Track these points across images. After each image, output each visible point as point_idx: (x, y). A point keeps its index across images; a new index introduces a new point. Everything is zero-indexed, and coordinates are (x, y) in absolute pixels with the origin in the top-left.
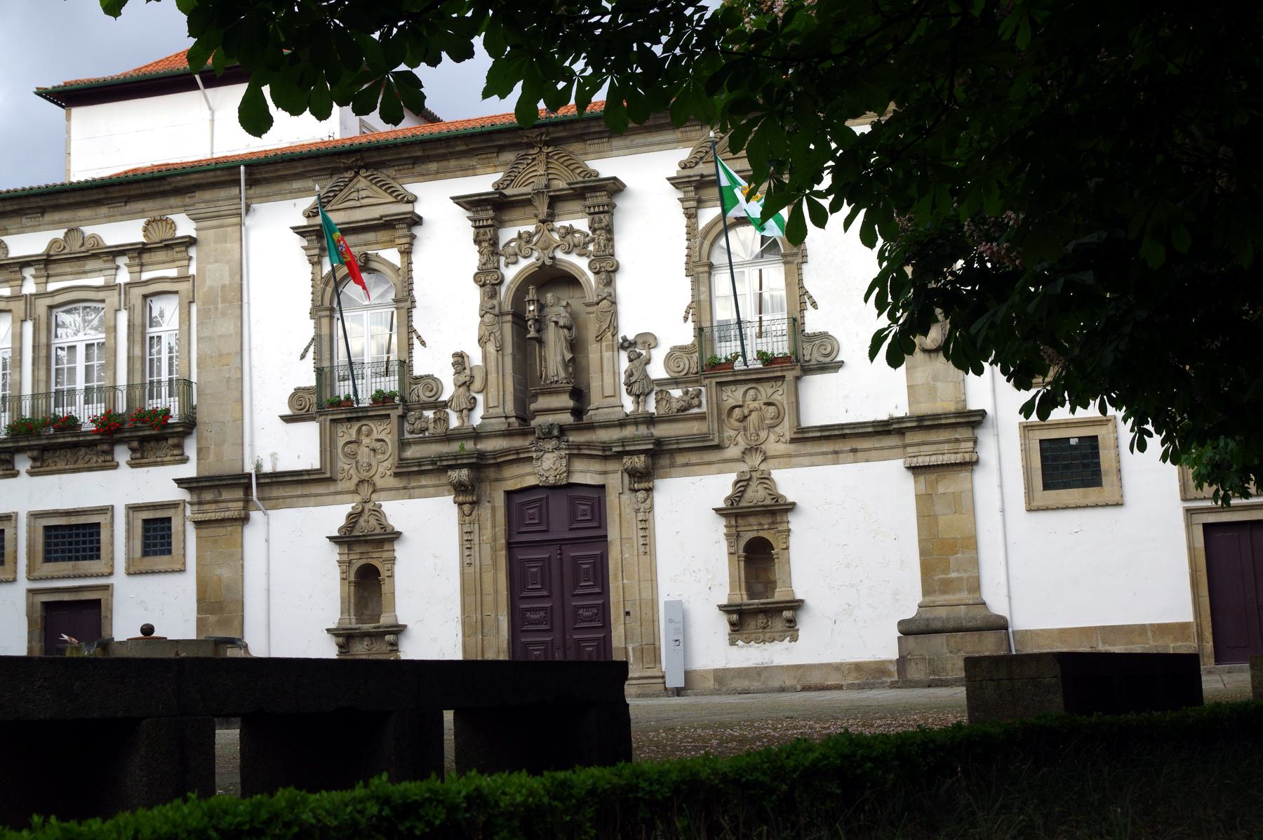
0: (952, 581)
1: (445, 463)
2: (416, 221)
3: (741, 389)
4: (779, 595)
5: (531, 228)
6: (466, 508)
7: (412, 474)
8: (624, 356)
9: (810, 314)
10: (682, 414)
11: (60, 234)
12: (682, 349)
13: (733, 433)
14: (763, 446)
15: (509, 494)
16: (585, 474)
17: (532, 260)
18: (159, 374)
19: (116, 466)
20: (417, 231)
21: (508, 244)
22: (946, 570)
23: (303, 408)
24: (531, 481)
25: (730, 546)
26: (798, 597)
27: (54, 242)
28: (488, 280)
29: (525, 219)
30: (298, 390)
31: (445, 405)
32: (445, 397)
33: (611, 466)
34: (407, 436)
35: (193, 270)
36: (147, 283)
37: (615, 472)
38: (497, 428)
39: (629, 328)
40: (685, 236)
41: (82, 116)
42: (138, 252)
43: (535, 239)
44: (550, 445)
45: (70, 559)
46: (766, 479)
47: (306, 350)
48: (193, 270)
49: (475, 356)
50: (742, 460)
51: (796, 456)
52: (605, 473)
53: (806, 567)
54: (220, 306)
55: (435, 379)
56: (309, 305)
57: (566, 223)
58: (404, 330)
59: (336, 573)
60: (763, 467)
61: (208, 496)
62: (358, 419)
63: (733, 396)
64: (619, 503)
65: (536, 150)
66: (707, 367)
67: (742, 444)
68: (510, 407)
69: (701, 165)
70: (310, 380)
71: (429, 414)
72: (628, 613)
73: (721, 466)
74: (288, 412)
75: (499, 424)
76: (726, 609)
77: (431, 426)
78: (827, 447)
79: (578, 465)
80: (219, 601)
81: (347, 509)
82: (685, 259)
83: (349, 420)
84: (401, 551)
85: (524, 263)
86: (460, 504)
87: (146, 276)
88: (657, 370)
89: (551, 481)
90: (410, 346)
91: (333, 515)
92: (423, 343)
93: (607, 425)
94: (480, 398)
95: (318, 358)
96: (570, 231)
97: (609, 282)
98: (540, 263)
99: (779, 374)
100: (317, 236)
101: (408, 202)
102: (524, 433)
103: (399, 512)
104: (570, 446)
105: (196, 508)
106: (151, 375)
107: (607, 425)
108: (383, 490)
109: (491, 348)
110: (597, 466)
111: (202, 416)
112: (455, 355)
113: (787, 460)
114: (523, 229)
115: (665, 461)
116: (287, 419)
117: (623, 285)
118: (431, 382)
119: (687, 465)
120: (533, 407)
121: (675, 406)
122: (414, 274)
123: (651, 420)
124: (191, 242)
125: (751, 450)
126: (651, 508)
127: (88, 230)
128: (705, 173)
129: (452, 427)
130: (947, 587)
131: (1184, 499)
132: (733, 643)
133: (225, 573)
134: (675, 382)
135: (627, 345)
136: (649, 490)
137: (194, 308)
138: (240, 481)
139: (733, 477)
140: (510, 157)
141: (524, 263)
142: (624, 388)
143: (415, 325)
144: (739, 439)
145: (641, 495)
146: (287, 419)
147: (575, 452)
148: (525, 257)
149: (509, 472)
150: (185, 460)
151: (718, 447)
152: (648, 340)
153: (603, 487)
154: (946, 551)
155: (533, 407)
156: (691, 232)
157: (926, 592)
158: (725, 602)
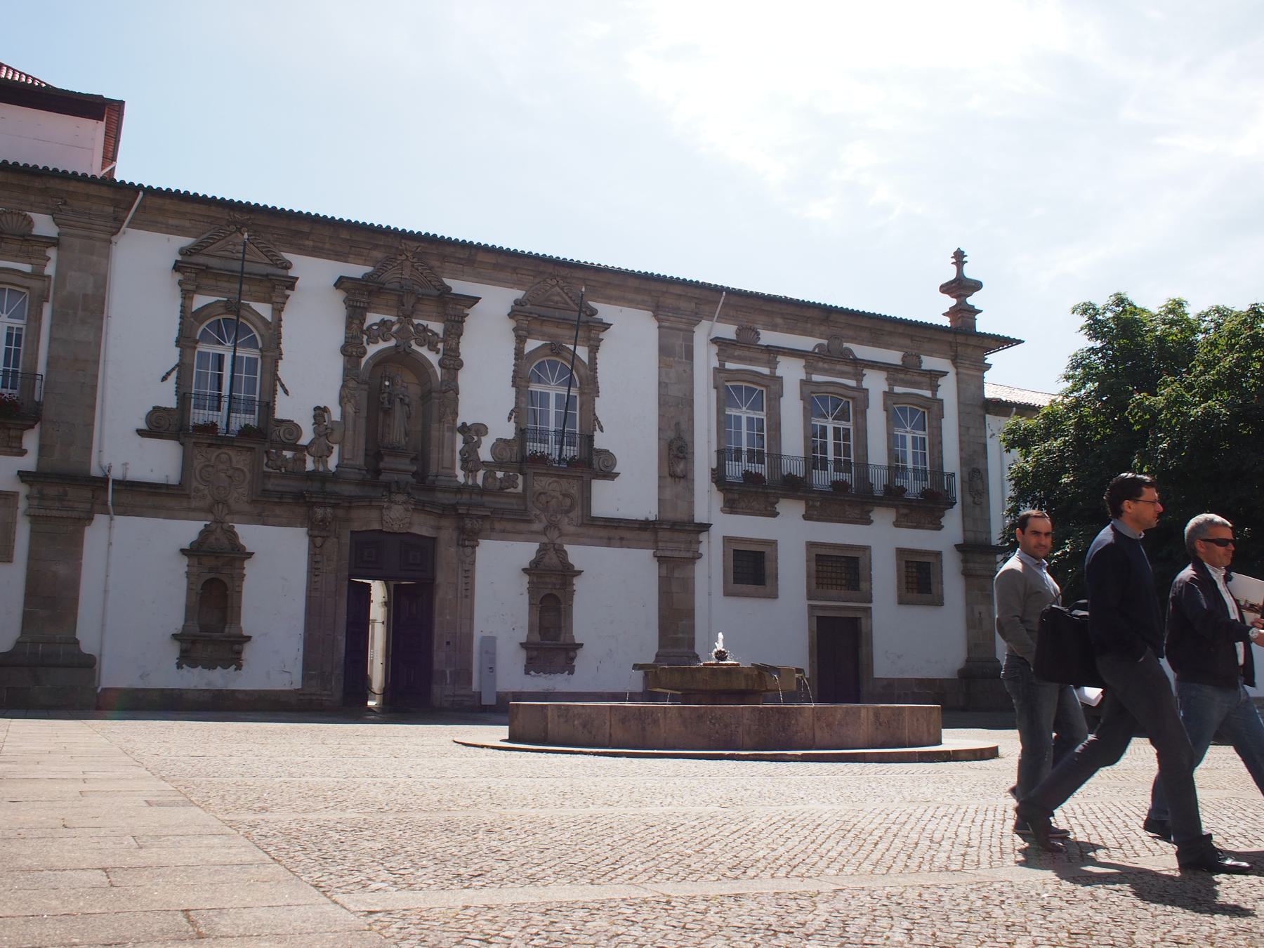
5: (394, 319)
6: (319, 541)
7: (271, 504)
8: (459, 439)
9: (597, 434)
10: (500, 492)
12: (505, 441)
13: (538, 512)
15: (352, 532)
16: (422, 526)
17: (392, 343)
20: (288, 292)
23: (159, 425)
24: (376, 526)
25: (531, 598)
26: (577, 641)
28: (351, 350)
30: (156, 409)
31: (306, 447)
33: (445, 522)
34: (266, 469)
35: (50, 270)
39: (466, 415)
43: (395, 328)
44: (400, 498)
46: (562, 554)
47: (168, 374)
48: (50, 270)
49: (336, 414)
50: (544, 532)
54: (80, 313)
56: (175, 334)
57: (424, 323)
59: (183, 584)
60: (558, 541)
61: (51, 491)
62: (219, 446)
63: (542, 483)
64: (447, 552)
65: (404, 257)
66: (520, 457)
68: (360, 461)
70: (170, 401)
71: (288, 454)
72: (448, 643)
74: (143, 426)
78: (604, 533)
81: (199, 526)
83: (210, 445)
84: (249, 567)
86: (310, 536)
88: (485, 454)
89: (396, 528)
90: (275, 391)
91: (188, 530)
92: (286, 392)
94: (336, 449)
96: (425, 329)
97: (455, 378)
100: (190, 271)
103: (249, 534)
105: (35, 502)
109: (350, 409)
113: (577, 540)
114: (387, 317)
115: (487, 525)
116: (140, 432)
117: (463, 378)
118: (294, 429)
119: (504, 531)
120: (382, 465)
123: (482, 491)
125: (552, 526)
131: (809, 598)
132: (527, 673)
133: (62, 570)
135: (464, 429)
136: (474, 547)
137: (47, 309)
139: (536, 546)
140: (378, 254)
142: (458, 464)
143: (281, 373)
145: (468, 550)
146: (140, 432)
148: (385, 341)
150: (22, 453)
151: (530, 522)
152: (481, 429)
153: (434, 539)
154: (676, 617)
155: (382, 465)
156: (519, 353)
157: (660, 647)
158: (524, 640)
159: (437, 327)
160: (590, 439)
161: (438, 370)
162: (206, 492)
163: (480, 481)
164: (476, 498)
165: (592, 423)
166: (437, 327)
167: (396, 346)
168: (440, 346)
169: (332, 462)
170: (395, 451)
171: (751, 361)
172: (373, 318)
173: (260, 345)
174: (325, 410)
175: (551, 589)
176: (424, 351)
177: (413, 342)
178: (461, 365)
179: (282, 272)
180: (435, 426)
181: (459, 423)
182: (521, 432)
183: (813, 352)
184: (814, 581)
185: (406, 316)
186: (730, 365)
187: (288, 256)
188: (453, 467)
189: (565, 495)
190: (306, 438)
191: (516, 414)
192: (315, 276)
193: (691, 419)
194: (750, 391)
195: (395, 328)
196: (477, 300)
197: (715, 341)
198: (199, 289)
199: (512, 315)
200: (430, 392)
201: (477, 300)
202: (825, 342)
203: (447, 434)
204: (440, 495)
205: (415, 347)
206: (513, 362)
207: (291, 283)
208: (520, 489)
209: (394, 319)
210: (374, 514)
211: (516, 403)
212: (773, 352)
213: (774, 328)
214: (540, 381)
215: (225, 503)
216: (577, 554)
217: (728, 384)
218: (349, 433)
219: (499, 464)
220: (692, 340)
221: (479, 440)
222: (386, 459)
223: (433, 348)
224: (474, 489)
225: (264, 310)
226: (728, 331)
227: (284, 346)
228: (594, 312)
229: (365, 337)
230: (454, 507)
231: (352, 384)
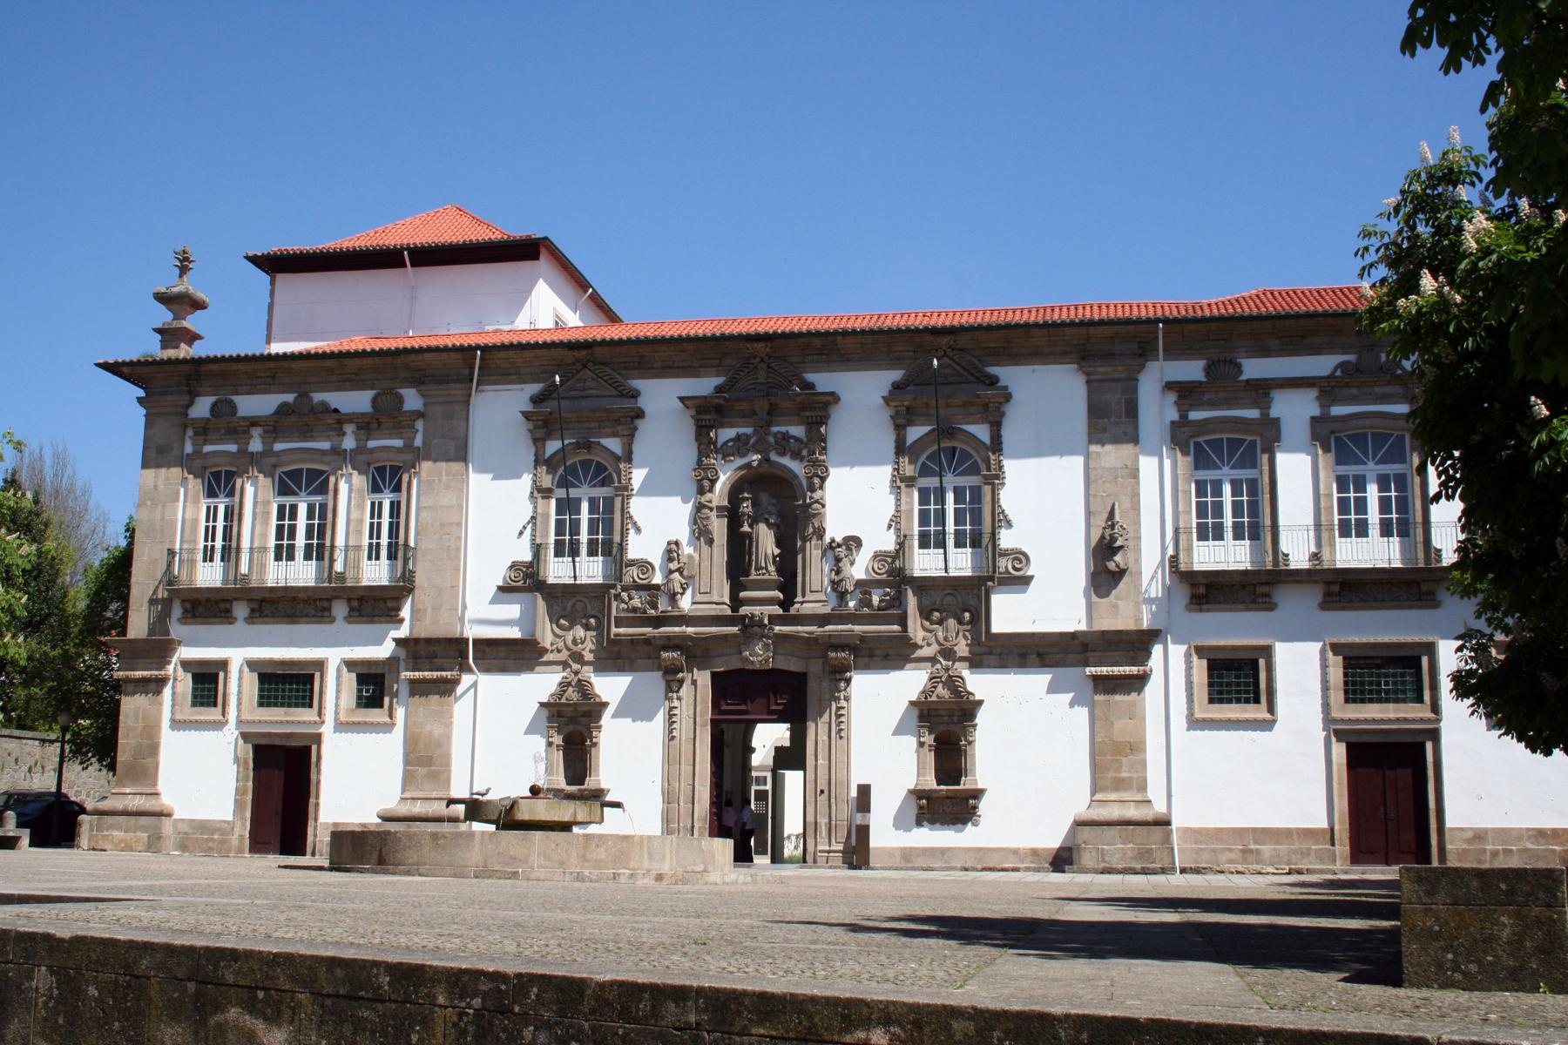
0: (1123, 780)
2: (640, 414)
4: (966, 784)
5: (749, 430)
11: (290, 398)
18: (379, 537)
19: (332, 620)
21: (726, 443)
22: (1118, 770)
27: (284, 405)
31: (657, 587)
32: (658, 579)
35: (418, 442)
36: (372, 451)
39: (835, 529)
41: (289, 283)
42: (367, 425)
45: (282, 705)
53: (990, 757)
57: (783, 429)
76: (917, 793)
80: (424, 760)
87: (372, 444)
91: (543, 684)
95: (533, 536)
96: (786, 437)
106: (371, 537)
111: (420, 580)
114: (742, 430)
118: (645, 566)
120: (743, 594)
124: (420, 415)
126: (847, 699)
127: (318, 397)
130: (1119, 784)
133: (435, 729)
135: (832, 546)
138: (456, 647)
152: (853, 543)
158: (912, 787)
159: (798, 431)
165: (1000, 520)
166: (798, 431)
171: (1229, 404)
174: (677, 543)
175: (946, 726)
176: (786, 461)
179: (628, 404)
181: (827, 539)
183: (1331, 376)
184: (1337, 696)
186: (1195, 415)
192: (662, 399)
193: (1136, 495)
194: (1234, 444)
197: (1169, 386)
198: (549, 435)
199: (887, 400)
202: (1351, 358)
209: (749, 430)
212: (1262, 390)
213: (1265, 352)
216: (978, 683)
217: (1200, 439)
220: (1134, 390)
226: (1192, 370)
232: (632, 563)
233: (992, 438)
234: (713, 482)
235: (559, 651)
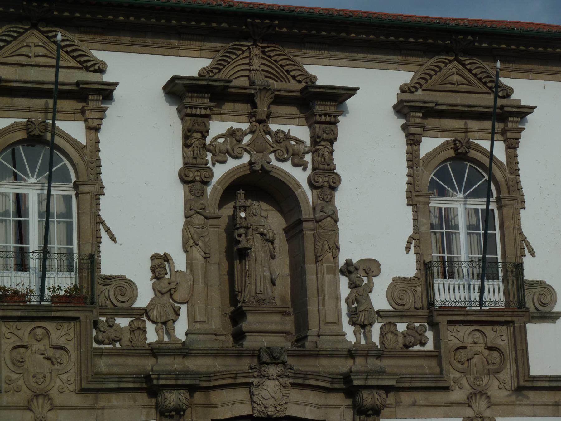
1: (162, 382)
3: (464, 330)
5: (245, 126)
8: (344, 281)
9: (528, 261)
10: (405, 351)
13: (458, 375)
14: (487, 391)
17: (246, 159)
24: (245, 410)
28: (193, 176)
29: (235, 116)
32: (142, 302)
37: (337, 407)
38: (209, 345)
39: (350, 250)
40: (405, 164)
43: (247, 139)
44: (273, 370)
49: (180, 262)
51: (520, 405)
52: (327, 407)
55: (130, 283)
57: (285, 128)
58: (87, 219)
67: (467, 389)
69: (420, 92)
71: (123, 322)
73: (447, 409)
75: (205, 342)
77: (126, 337)
79: (296, 395)
82: (405, 187)
85: (232, 164)
88: (379, 300)
92: (113, 238)
93: (332, 354)
94: (184, 309)
96: (287, 137)
97: (330, 200)
98: (257, 167)
99: (509, 319)
101: (95, 71)
102: (240, 355)
104: (296, 375)
107: (332, 354)
108: (63, 407)
109: (197, 254)
110: (313, 397)
112: (154, 257)
115: (391, 398)
118: (125, 286)
119: (414, 405)
120: (245, 326)
121: (401, 340)
122: (101, 155)
125: (479, 393)
128: (440, 101)
129: (149, 341)
134: (402, 316)
141: (232, 164)
143: (104, 214)
144: (464, 382)
147: (300, 381)
149: (216, 397)
151: (446, 389)
152: (371, 267)
156: (412, 159)
160: (519, 267)
161: (309, 193)
162: (21, 382)
163: (376, 338)
164: (374, 363)
165: (520, 245)
166: (301, 132)
167: (251, 163)
168: (308, 158)
169: (181, 329)
170: (263, 307)
172: (218, 128)
173: (74, 179)
174: (166, 258)
176: (287, 167)
177: (272, 156)
178: (338, 179)
180: (310, 267)
181: (342, 261)
182: (425, 267)
185: (260, 122)
187: (100, 55)
188: (338, 322)
189: (490, 348)
190: (144, 298)
191: (416, 241)
195: (247, 139)
196: (352, 91)
200: (300, 222)
201: (352, 91)
203: (328, 277)
204: (325, 362)
205: (274, 162)
206: (406, 171)
207: (106, 93)
208: (430, 346)
209: (245, 126)
210: (242, 394)
211: (415, 226)
214: (442, 193)
215: (45, 395)
218: (200, 286)
219: (401, 314)
221: (370, 281)
222: (250, 318)
223: (299, 164)
224: (369, 352)
225: (74, 129)
227: (107, 175)
228: (508, 92)
229: (209, 155)
230: (347, 378)
231: (198, 220)
232: (108, 279)
233: (508, 157)
234: (206, 183)
235: (18, 391)
